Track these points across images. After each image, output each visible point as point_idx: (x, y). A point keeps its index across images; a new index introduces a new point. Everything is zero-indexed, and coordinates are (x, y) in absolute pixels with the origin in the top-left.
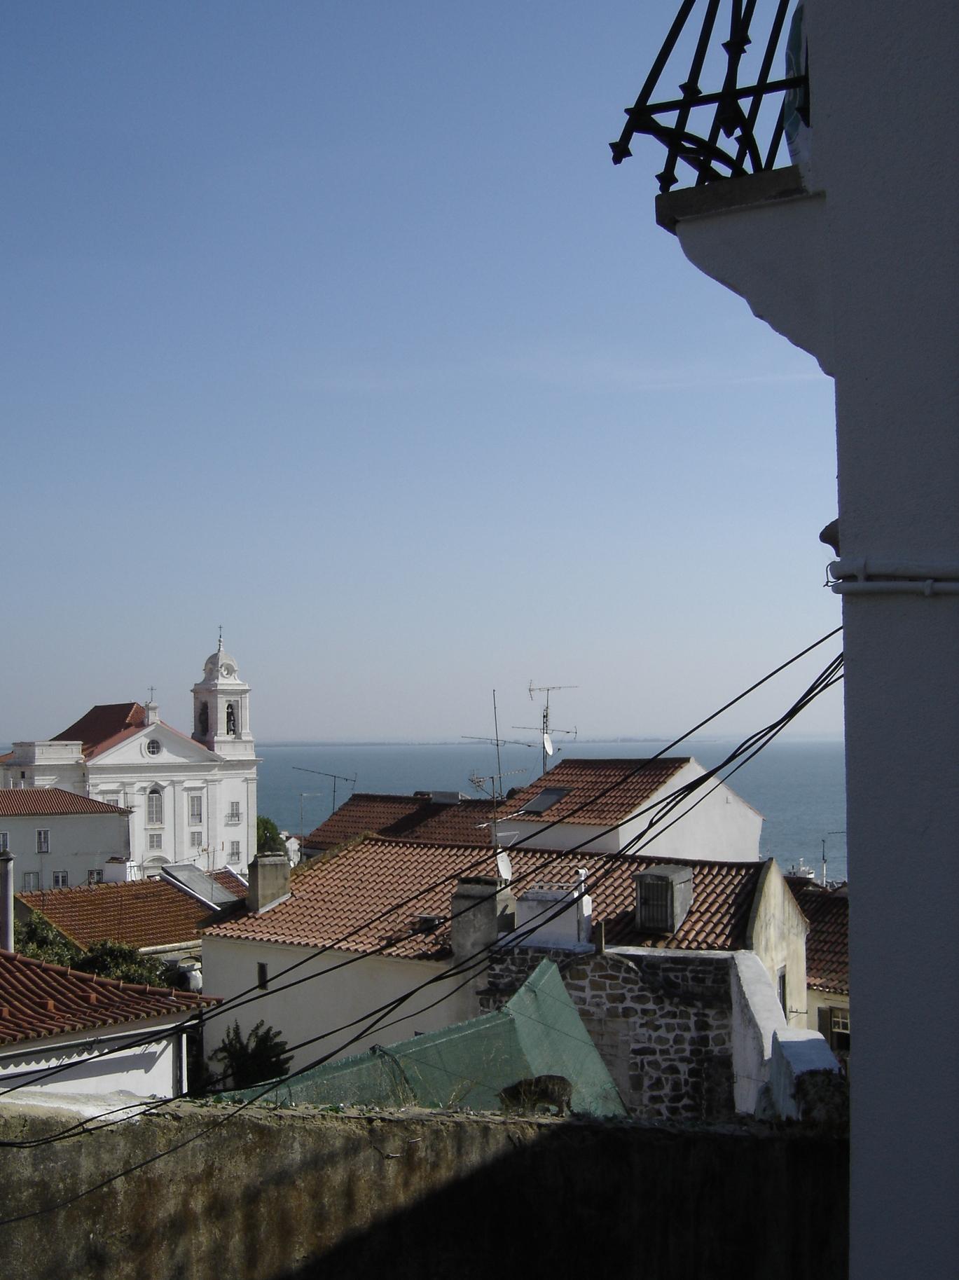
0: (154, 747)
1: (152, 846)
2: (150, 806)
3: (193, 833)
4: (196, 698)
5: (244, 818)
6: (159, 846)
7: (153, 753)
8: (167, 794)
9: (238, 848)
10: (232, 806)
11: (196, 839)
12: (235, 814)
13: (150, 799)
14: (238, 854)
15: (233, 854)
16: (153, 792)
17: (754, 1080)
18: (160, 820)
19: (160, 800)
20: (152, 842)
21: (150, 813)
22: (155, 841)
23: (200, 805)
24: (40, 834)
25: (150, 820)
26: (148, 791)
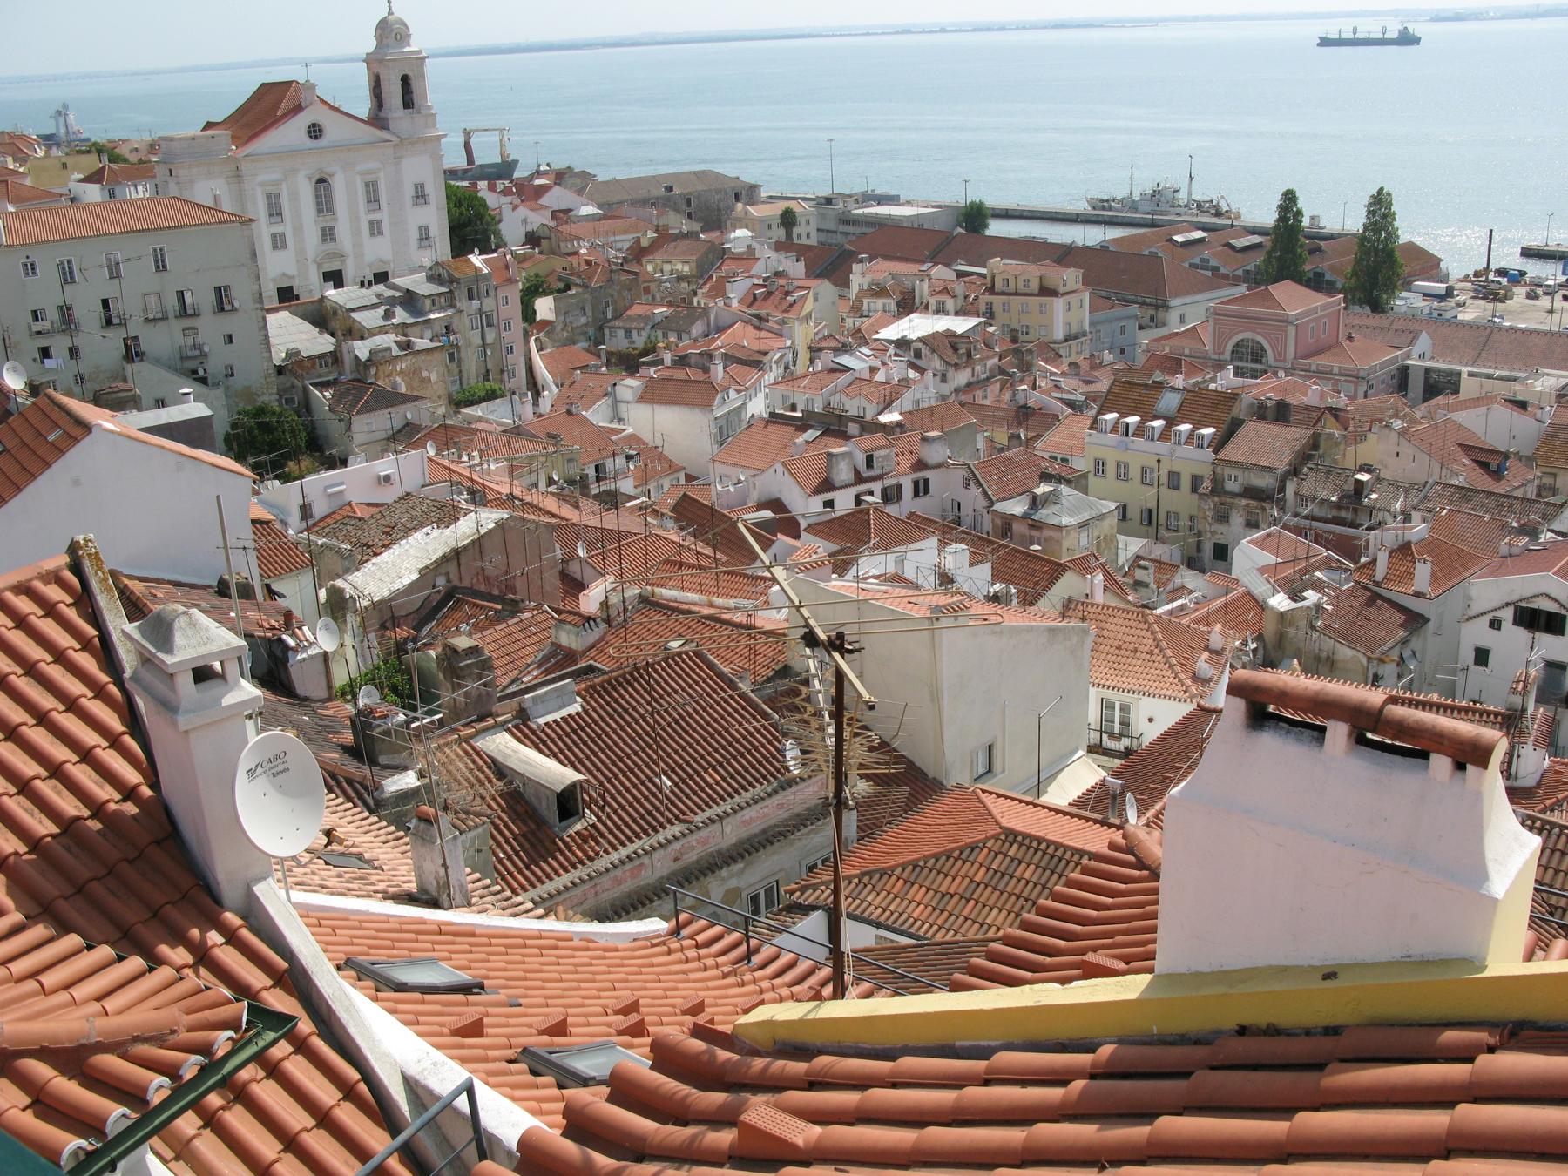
0: (315, 131)
1: (324, 240)
2: (317, 197)
3: (371, 223)
4: (368, 69)
5: (433, 198)
6: (333, 239)
7: (316, 138)
8: (339, 186)
9: (427, 234)
10: (416, 187)
11: (376, 229)
12: (420, 196)
13: (316, 190)
14: (428, 238)
15: (421, 239)
16: (321, 181)
17: (162, 906)
18: (331, 210)
19: (329, 190)
20: (324, 235)
21: (318, 204)
22: (328, 234)
23: (376, 191)
24: (155, 250)
25: (320, 211)
26: (314, 180)
